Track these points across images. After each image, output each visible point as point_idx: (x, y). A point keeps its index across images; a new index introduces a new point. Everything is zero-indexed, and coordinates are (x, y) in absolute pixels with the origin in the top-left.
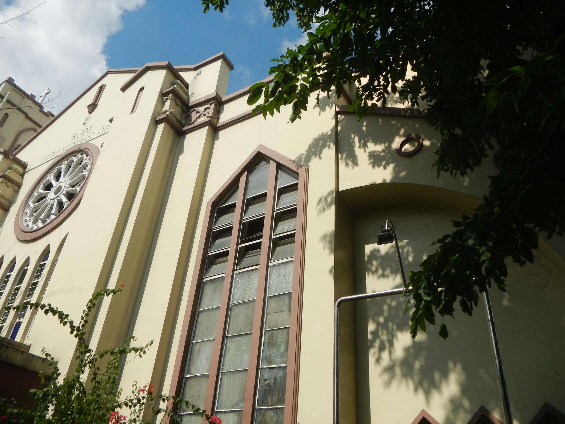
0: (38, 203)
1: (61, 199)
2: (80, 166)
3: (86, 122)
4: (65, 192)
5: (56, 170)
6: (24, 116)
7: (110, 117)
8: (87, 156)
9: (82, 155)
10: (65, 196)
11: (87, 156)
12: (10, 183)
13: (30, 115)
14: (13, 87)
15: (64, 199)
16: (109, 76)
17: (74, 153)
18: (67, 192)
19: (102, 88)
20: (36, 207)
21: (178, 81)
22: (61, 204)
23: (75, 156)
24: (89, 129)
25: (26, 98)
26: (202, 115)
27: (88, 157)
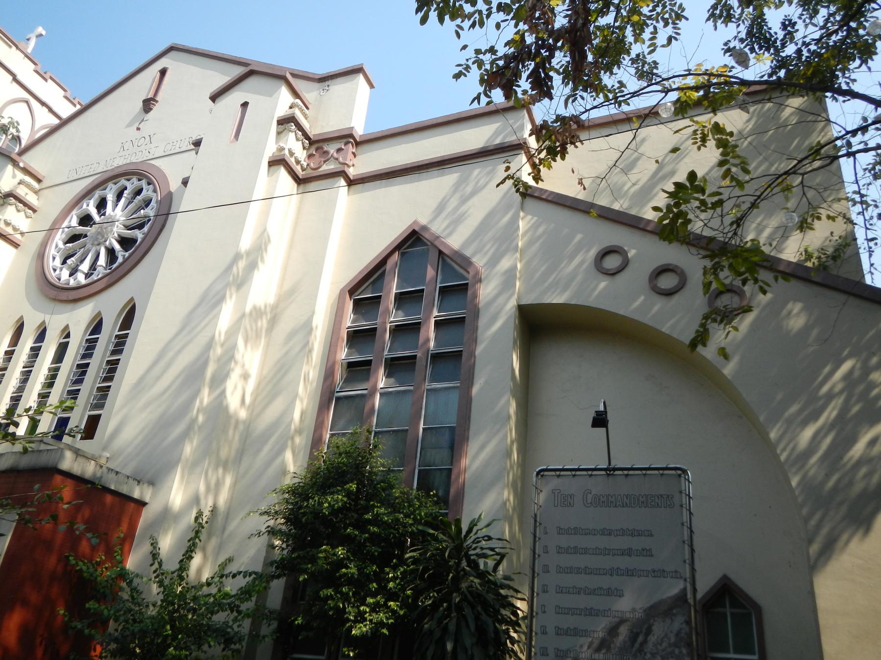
0: (71, 245)
1: (110, 244)
2: (139, 198)
3: (140, 126)
4: (116, 235)
5: (97, 194)
6: (11, 78)
7: (195, 137)
8: (149, 184)
9: (139, 180)
10: (116, 240)
11: (149, 184)
12: (21, 205)
13: (19, 77)
15: (117, 247)
16: (173, 54)
17: (127, 174)
18: (119, 235)
19: (163, 72)
20: (69, 250)
21: (298, 101)
22: (111, 253)
23: (128, 180)
24: (148, 138)
25: (14, 48)
26: (332, 159)
27: (151, 186)
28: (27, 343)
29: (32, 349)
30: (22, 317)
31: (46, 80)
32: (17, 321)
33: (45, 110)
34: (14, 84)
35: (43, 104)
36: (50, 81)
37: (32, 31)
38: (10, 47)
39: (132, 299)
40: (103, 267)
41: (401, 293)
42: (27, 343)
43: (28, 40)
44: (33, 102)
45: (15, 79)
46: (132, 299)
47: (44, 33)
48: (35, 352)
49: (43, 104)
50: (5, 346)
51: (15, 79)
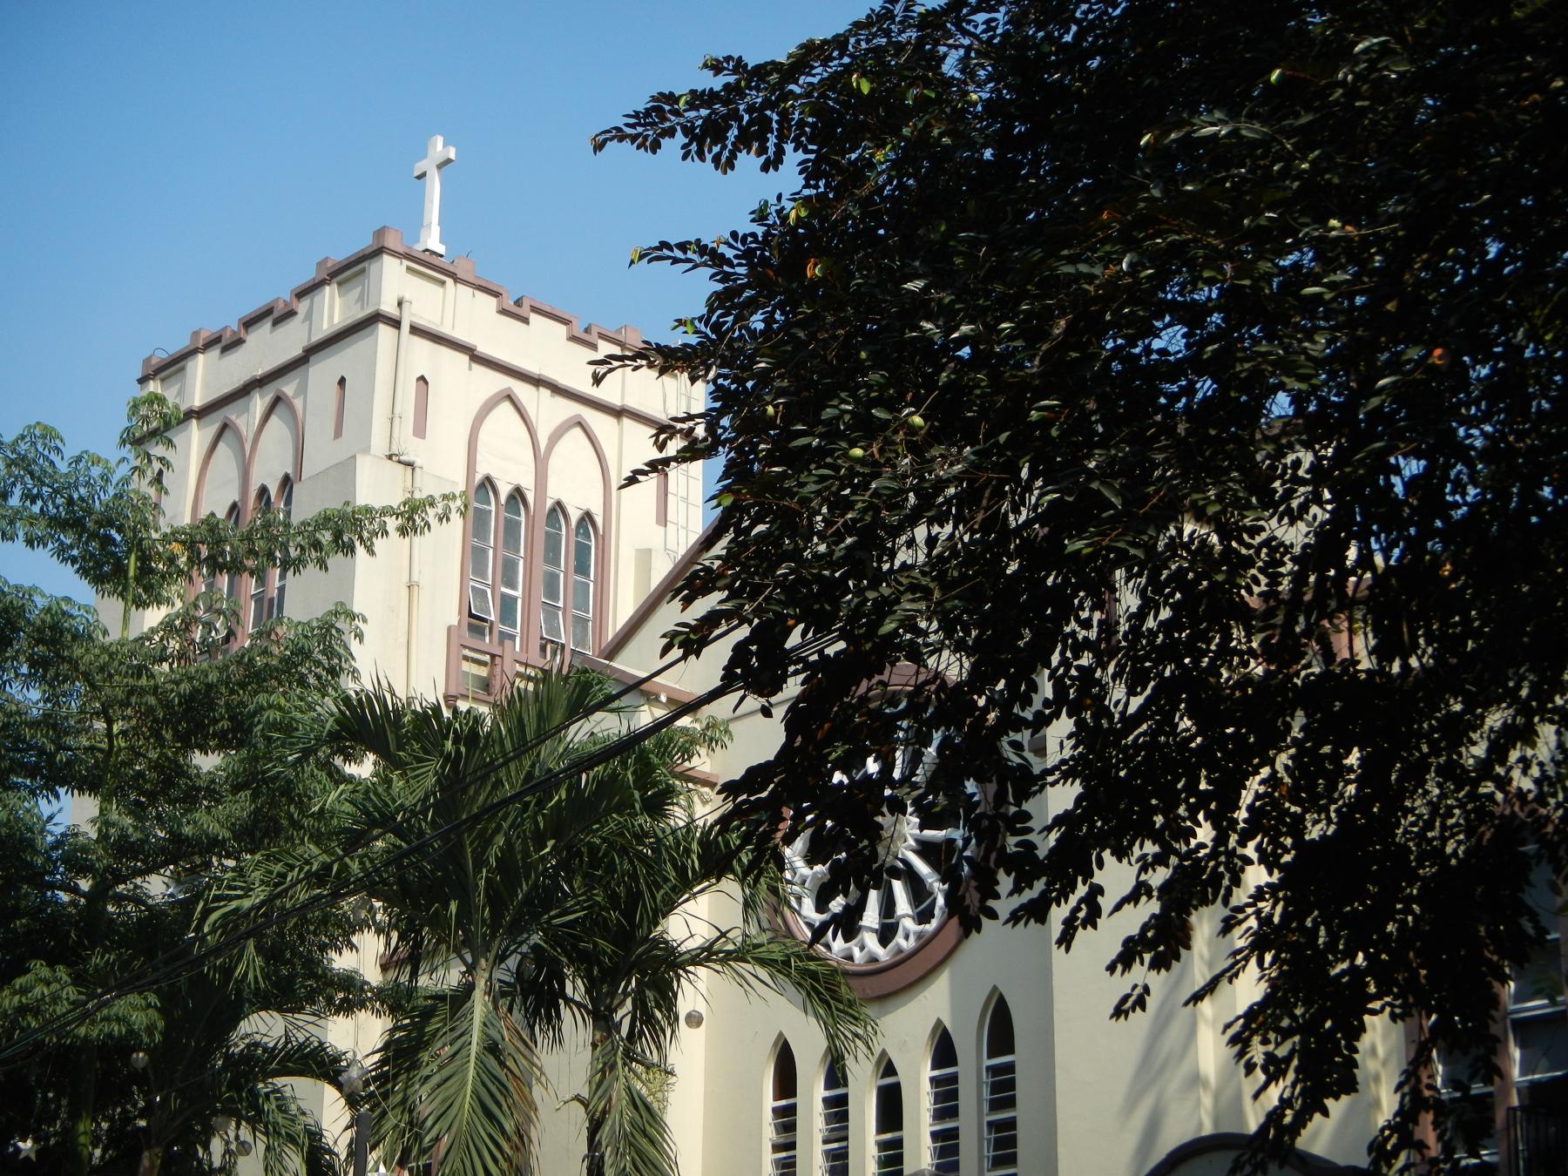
6: (464, 359)
13: (483, 349)
14: (406, 263)
25: (450, 281)
28: (813, 1092)
29: (828, 1102)
30: (781, 1034)
31: (526, 321)
32: (775, 1044)
33: (545, 393)
34: (474, 366)
35: (537, 382)
36: (533, 317)
37: (425, 156)
38: (443, 283)
39: (995, 988)
40: (909, 916)
41: (1534, 1085)
42: (813, 1092)
43: (422, 176)
44: (523, 391)
45: (476, 358)
46: (995, 988)
47: (452, 156)
48: (838, 1109)
49: (537, 382)
50: (769, 1102)
51: (476, 358)
